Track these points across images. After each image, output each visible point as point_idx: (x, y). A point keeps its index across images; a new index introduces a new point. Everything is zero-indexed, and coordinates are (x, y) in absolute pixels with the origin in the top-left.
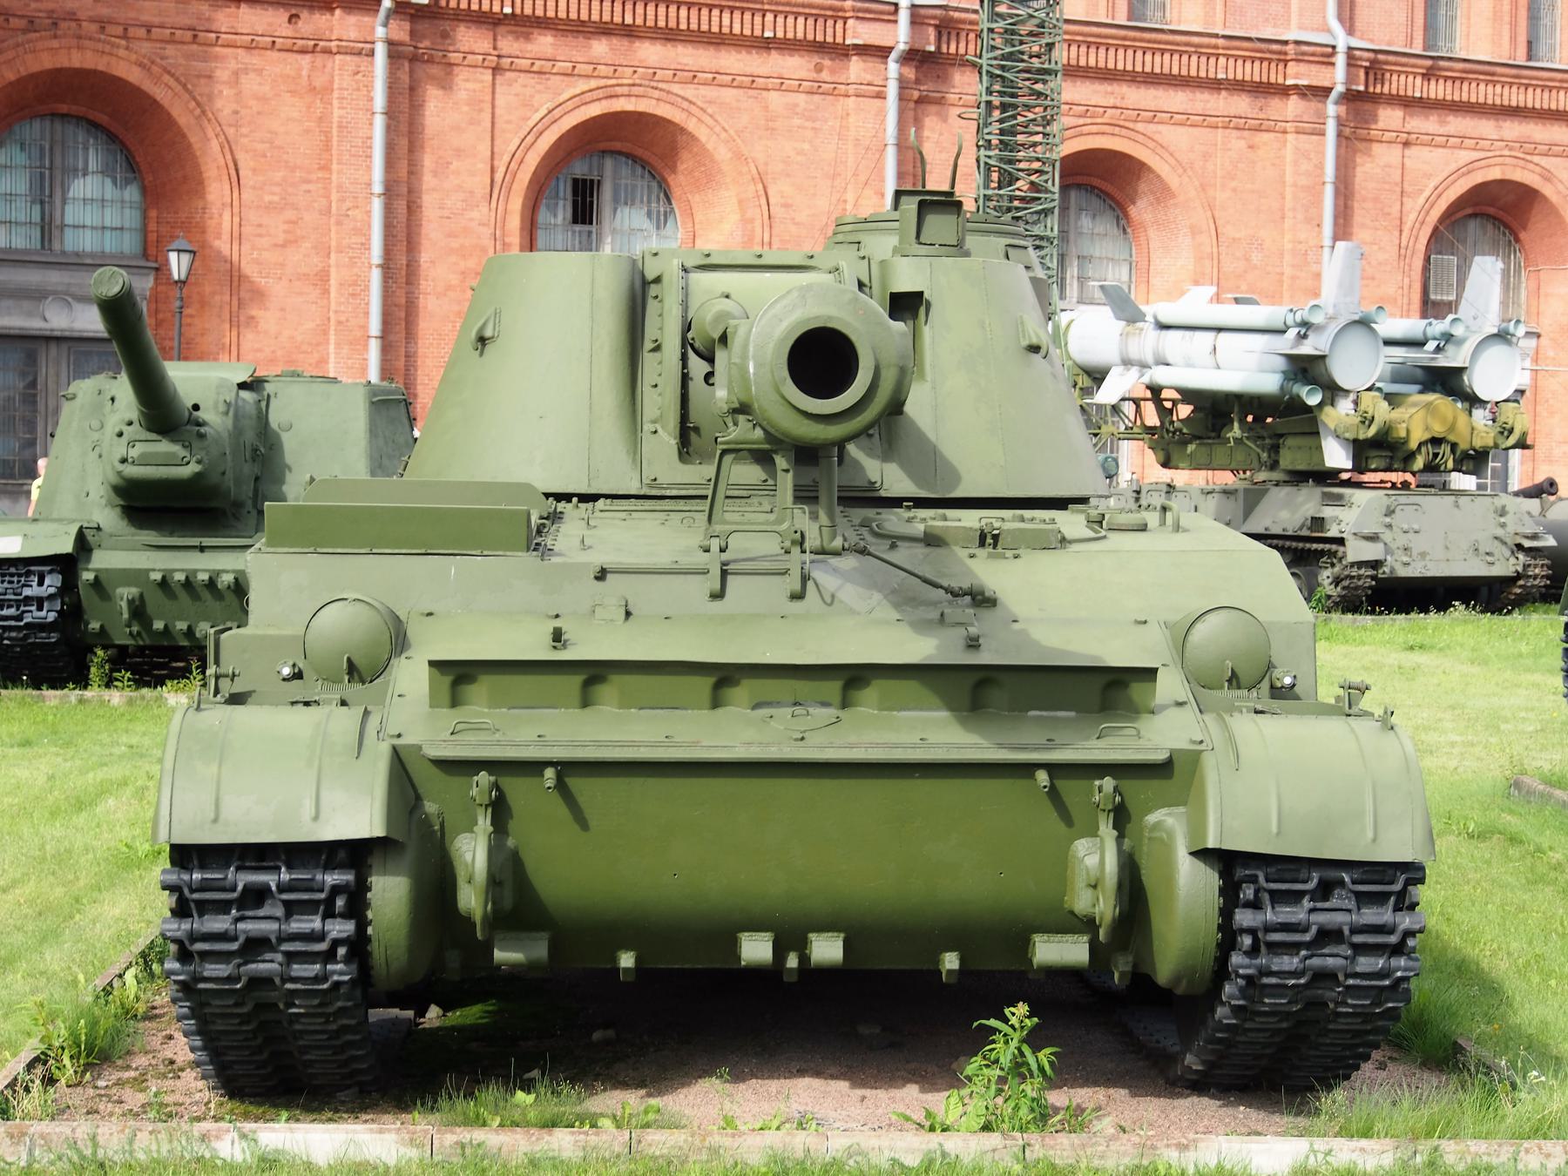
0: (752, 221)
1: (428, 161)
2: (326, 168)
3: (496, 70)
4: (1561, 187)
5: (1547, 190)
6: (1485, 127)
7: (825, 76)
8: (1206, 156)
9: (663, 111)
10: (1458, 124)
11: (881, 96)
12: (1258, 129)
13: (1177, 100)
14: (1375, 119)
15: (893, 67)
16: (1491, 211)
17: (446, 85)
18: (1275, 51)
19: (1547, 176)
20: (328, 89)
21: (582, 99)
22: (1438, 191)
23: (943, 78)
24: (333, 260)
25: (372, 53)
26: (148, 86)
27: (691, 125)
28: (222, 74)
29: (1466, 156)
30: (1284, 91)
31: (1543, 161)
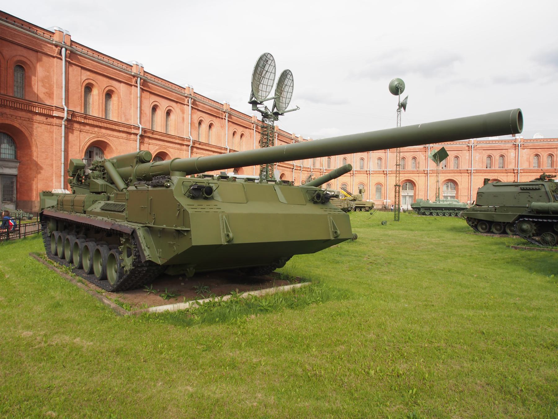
1: (70, 146)
2: (52, 146)
3: (80, 131)
6: (204, 152)
9: (105, 140)
10: (202, 151)
11: (136, 141)
15: (138, 137)
17: (73, 133)
18: (183, 139)
20: (53, 132)
21: (94, 138)
24: (54, 162)
25: (61, 126)
26: (20, 128)
27: (110, 143)
28: (34, 128)
30: (183, 145)
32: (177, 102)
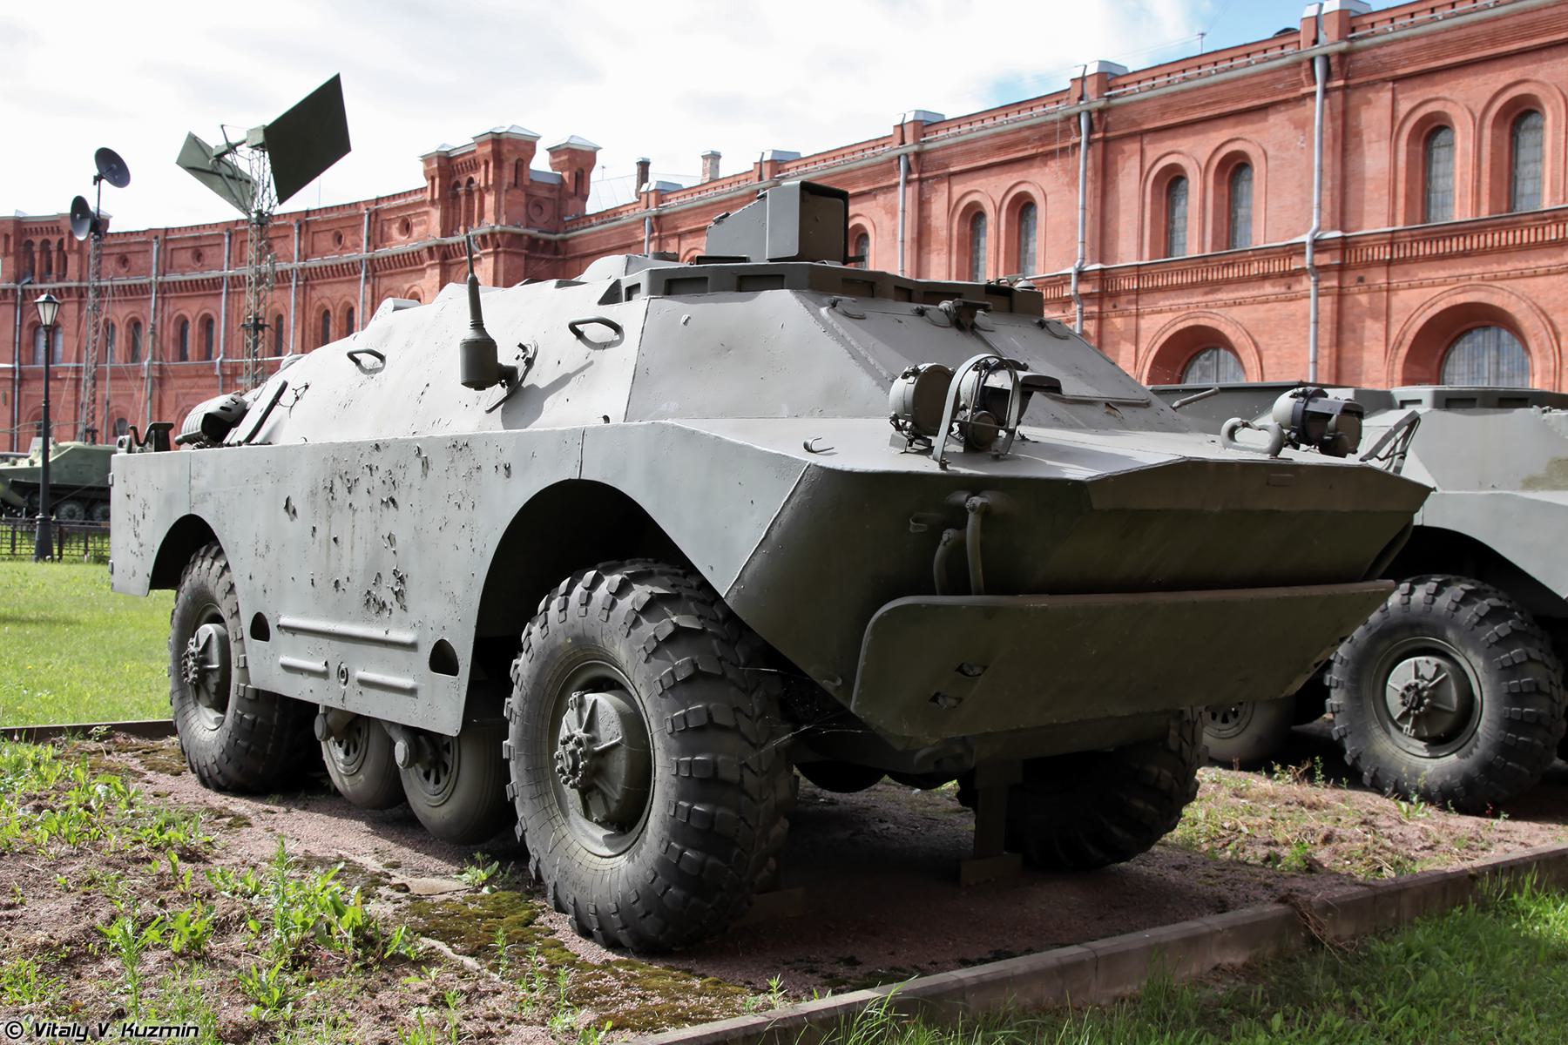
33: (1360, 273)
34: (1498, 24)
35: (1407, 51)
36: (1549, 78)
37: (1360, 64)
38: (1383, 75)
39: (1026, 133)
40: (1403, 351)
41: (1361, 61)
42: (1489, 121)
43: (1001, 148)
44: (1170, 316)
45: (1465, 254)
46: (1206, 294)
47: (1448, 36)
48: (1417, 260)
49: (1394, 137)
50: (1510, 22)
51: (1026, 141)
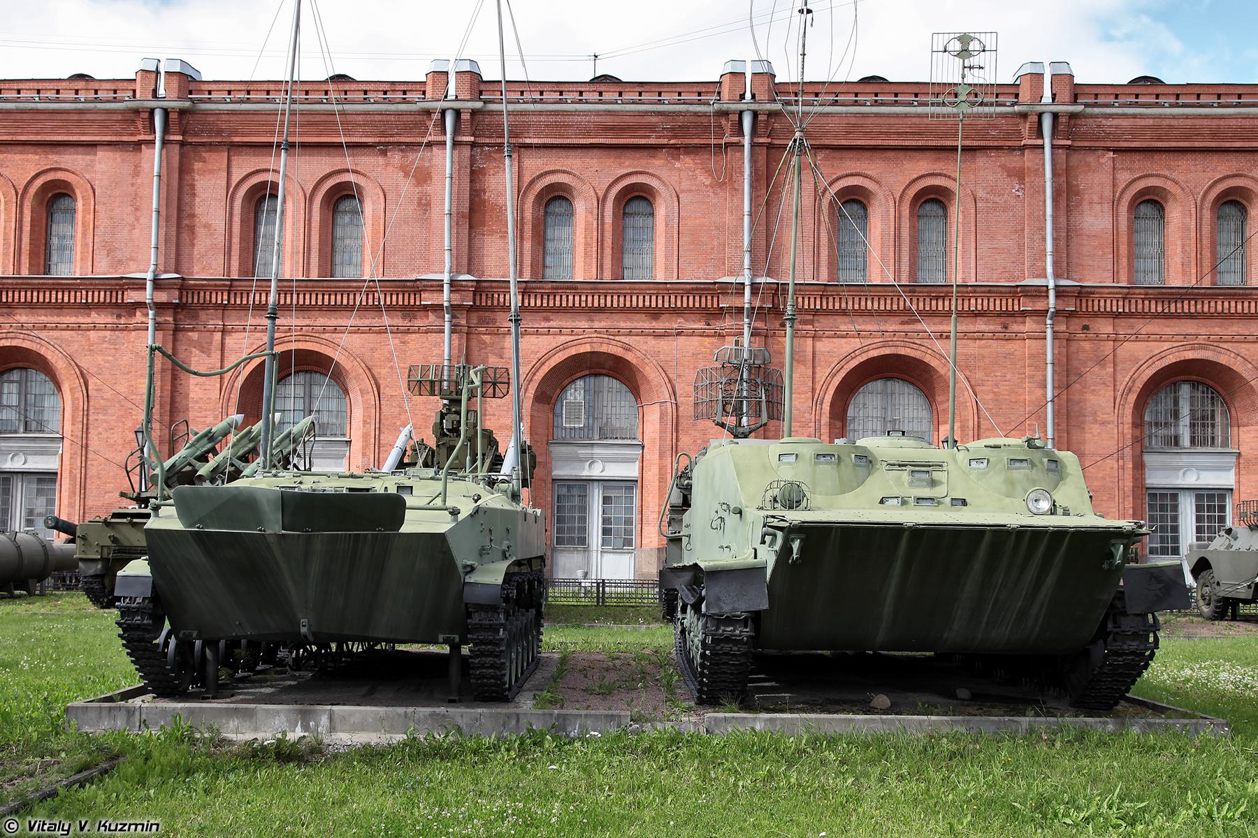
0: (78, 399)
4: (638, 354)
5: (629, 357)
7: (122, 321)
8: (372, 350)
9: (26, 345)
12: (408, 332)
13: (352, 321)
14: (494, 321)
16: (604, 371)
18: (417, 287)
19: (628, 348)
22: (541, 362)
23: (196, 317)
29: (563, 339)
31: (623, 339)
32: (382, 148)
33: (1086, 322)
34: (1222, 122)
35: (1133, 127)
36: (1257, 175)
37: (1083, 129)
38: (1108, 144)
39: (654, 119)
40: (1132, 398)
41: (1086, 126)
42: (1208, 205)
43: (607, 129)
44: (856, 343)
45: (1191, 316)
46: (903, 323)
47: (1174, 122)
48: (1143, 315)
49: (1115, 203)
50: (1232, 122)
51: (652, 128)
